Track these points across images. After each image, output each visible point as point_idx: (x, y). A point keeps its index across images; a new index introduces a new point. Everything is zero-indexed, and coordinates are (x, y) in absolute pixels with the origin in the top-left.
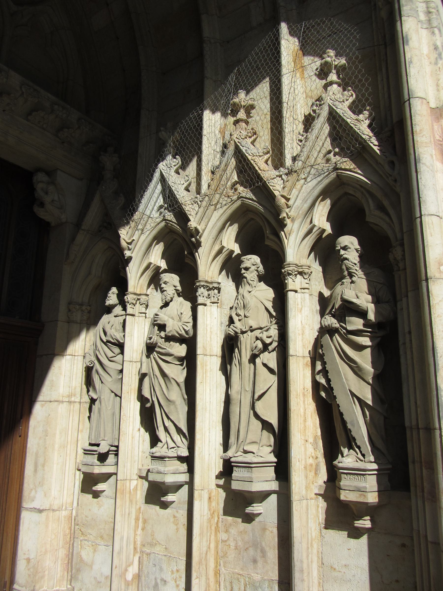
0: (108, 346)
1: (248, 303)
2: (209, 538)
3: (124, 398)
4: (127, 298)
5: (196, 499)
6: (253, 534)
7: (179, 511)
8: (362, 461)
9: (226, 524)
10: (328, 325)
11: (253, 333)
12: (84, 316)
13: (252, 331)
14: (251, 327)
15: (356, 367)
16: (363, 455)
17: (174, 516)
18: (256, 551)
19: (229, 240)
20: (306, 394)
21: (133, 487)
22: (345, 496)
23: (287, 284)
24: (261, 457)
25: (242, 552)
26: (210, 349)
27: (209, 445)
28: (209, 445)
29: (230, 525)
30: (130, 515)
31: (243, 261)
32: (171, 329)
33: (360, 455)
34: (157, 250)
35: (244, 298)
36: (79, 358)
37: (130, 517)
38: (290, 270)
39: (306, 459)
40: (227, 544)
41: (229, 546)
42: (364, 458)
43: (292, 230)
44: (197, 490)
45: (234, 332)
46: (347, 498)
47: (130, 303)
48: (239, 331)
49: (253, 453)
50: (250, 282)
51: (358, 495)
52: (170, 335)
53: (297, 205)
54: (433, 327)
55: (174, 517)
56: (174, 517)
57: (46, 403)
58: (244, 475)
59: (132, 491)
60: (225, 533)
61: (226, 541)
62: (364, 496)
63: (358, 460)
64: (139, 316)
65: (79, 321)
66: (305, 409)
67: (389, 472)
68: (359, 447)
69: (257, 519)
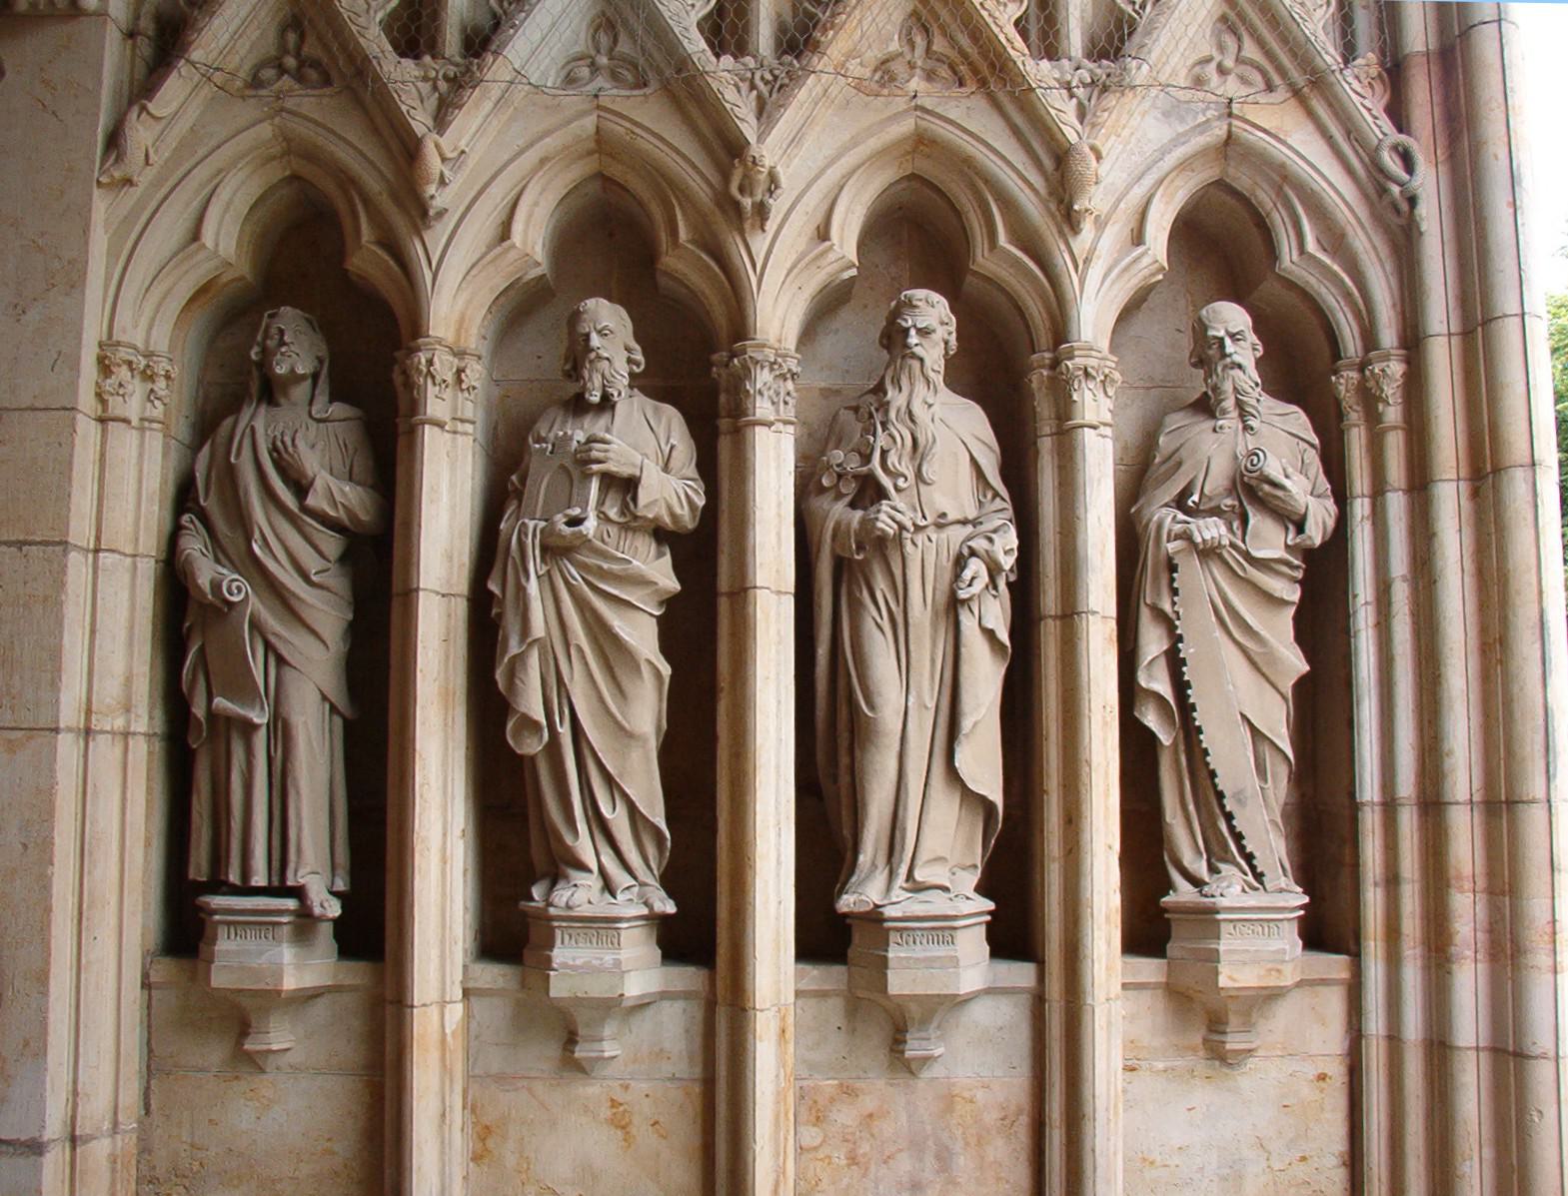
0: (308, 529)
1: (931, 440)
2: (782, 1146)
3: (423, 724)
4: (430, 362)
5: (760, 1037)
6: (910, 1117)
7: (633, 1084)
8: (1256, 889)
9: (815, 1102)
10: (1212, 538)
11: (944, 535)
12: (156, 402)
13: (940, 526)
14: (943, 515)
15: (1265, 654)
16: (1259, 876)
17: (612, 1100)
18: (921, 1160)
19: (846, 228)
20: (1109, 719)
21: (454, 1027)
22: (1231, 978)
23: (1079, 404)
24: (968, 898)
25: (873, 1168)
26: (777, 571)
27: (778, 875)
28: (778, 875)
29: (832, 1100)
30: (448, 1118)
31: (916, 307)
32: (658, 496)
33: (1250, 878)
34: (536, 204)
35: (913, 421)
36: (139, 565)
37: (447, 1122)
38: (1092, 368)
39: (1107, 894)
40: (822, 1156)
41: (827, 1161)
42: (1262, 883)
43: (1097, 253)
44: (762, 1011)
45: (895, 526)
46: (1234, 980)
47: (438, 379)
48: (909, 524)
49: (946, 889)
50: (932, 374)
51: (1262, 972)
52: (650, 516)
53: (1113, 184)
54: (1544, 575)
55: (614, 1103)
56: (614, 1103)
57: (30, 738)
58: (929, 954)
59: (449, 1038)
60: (814, 1125)
61: (816, 1149)
62: (1278, 971)
63: (1247, 889)
64: (455, 432)
65: (135, 422)
66: (1108, 763)
67: (1302, 912)
68: (1249, 858)
69: (925, 1074)
